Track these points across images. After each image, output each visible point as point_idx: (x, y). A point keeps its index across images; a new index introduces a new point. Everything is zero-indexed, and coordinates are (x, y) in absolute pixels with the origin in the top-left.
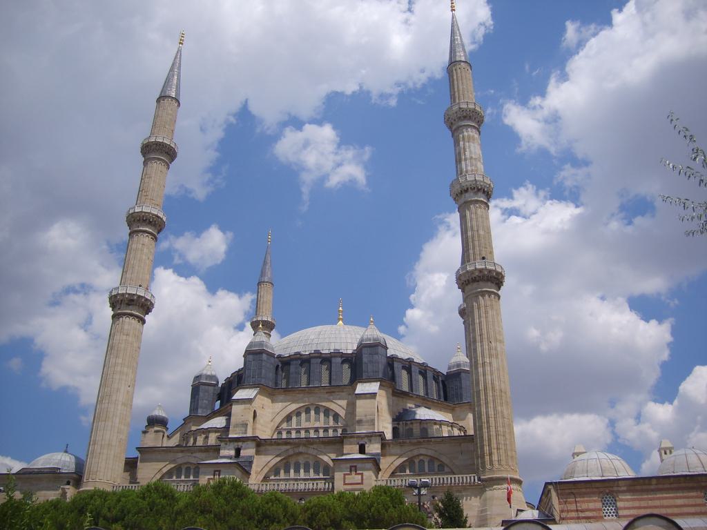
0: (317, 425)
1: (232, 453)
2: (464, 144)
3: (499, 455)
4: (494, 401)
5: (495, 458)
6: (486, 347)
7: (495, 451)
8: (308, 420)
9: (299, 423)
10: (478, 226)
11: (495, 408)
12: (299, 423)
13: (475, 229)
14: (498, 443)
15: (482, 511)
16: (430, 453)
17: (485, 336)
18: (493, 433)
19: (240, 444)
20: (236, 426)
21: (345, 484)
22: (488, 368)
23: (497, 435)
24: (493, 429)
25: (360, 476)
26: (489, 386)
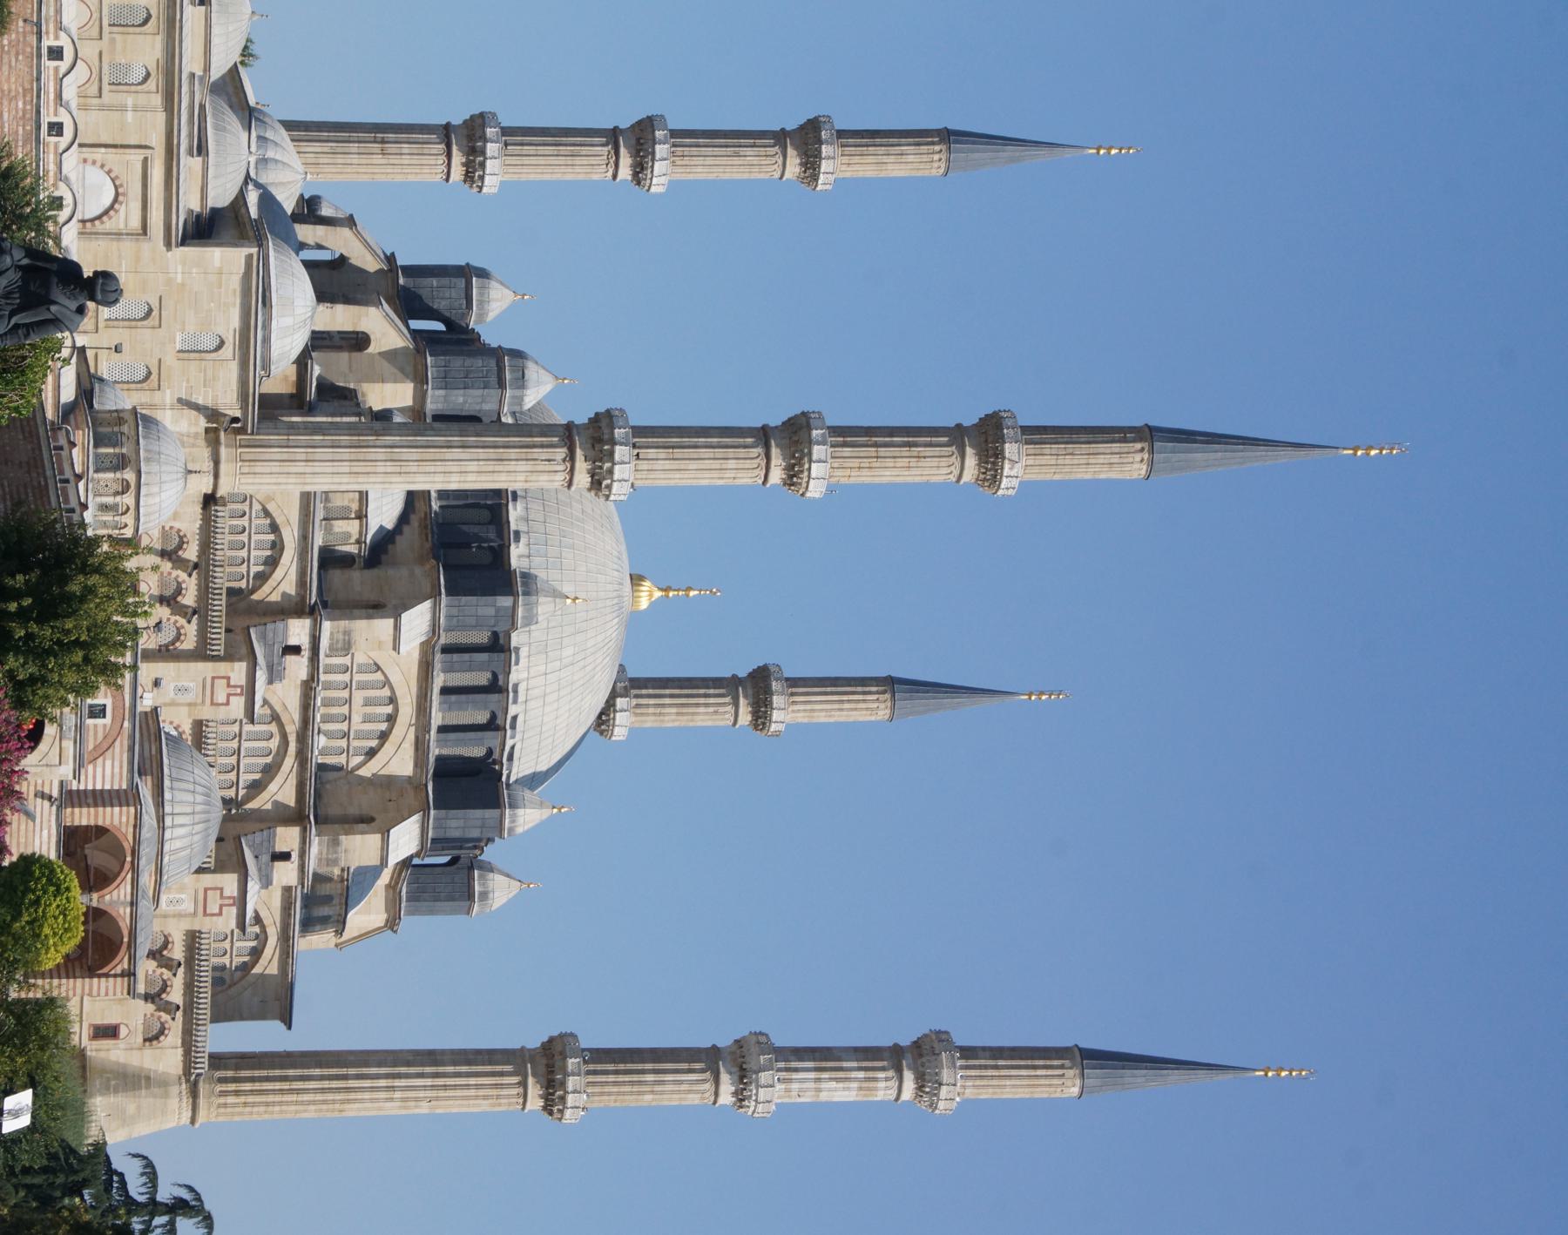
0: (356, 718)
1: (292, 641)
2: (856, 1079)
3: (235, 1105)
4: (324, 1102)
5: (231, 1100)
6: (421, 1094)
7: (242, 1099)
8: (368, 702)
9: (363, 686)
10: (662, 1093)
11: (310, 1103)
12: (363, 686)
13: (658, 1088)
14: (254, 1104)
15: (148, 1078)
16: (268, 952)
17: (442, 1094)
18: (271, 1098)
19: (306, 653)
20: (347, 633)
21: (206, 890)
22: (382, 1095)
23: (267, 1104)
24: (278, 1098)
25: (217, 911)
26: (352, 1096)
